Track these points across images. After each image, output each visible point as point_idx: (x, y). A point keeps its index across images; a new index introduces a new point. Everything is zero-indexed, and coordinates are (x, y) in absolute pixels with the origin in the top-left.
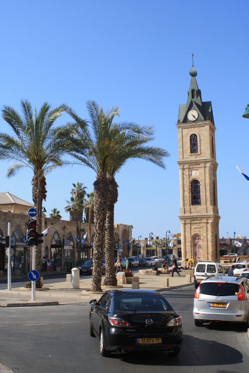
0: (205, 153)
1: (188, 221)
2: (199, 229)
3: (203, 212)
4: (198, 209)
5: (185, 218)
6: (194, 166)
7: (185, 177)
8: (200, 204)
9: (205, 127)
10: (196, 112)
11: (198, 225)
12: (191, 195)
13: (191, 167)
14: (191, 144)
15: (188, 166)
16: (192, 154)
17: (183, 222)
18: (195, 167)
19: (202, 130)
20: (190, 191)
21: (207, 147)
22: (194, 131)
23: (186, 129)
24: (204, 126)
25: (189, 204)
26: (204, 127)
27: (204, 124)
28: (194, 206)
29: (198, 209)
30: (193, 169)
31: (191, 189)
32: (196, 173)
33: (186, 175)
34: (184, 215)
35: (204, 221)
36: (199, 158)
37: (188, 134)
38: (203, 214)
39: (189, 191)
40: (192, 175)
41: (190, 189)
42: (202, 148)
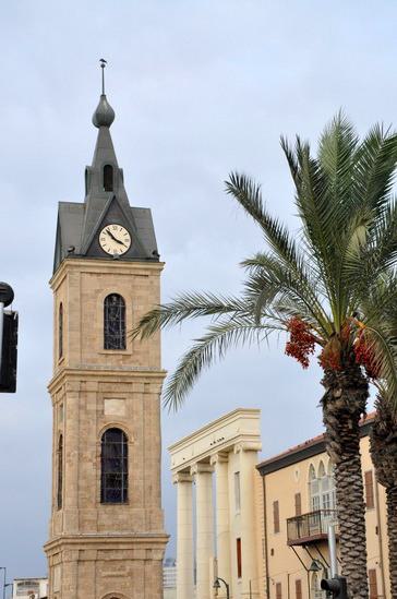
0: (148, 352)
1: (91, 554)
2: (120, 580)
3: (135, 528)
5: (83, 544)
6: (114, 386)
7: (83, 417)
8: (126, 500)
9: (152, 278)
10: (125, 231)
11: (118, 566)
12: (99, 472)
13: (104, 387)
14: (105, 325)
16: (111, 352)
17: (75, 556)
18: (117, 390)
20: (99, 459)
22: (119, 286)
23: (95, 277)
25: (94, 501)
26: (147, 280)
27: (146, 269)
28: (110, 508)
29: (121, 517)
30: (109, 395)
31: (102, 455)
32: (118, 410)
33: (87, 413)
34: (76, 532)
35: (140, 554)
36: (128, 366)
37: (98, 291)
40: (106, 413)
41: (99, 454)
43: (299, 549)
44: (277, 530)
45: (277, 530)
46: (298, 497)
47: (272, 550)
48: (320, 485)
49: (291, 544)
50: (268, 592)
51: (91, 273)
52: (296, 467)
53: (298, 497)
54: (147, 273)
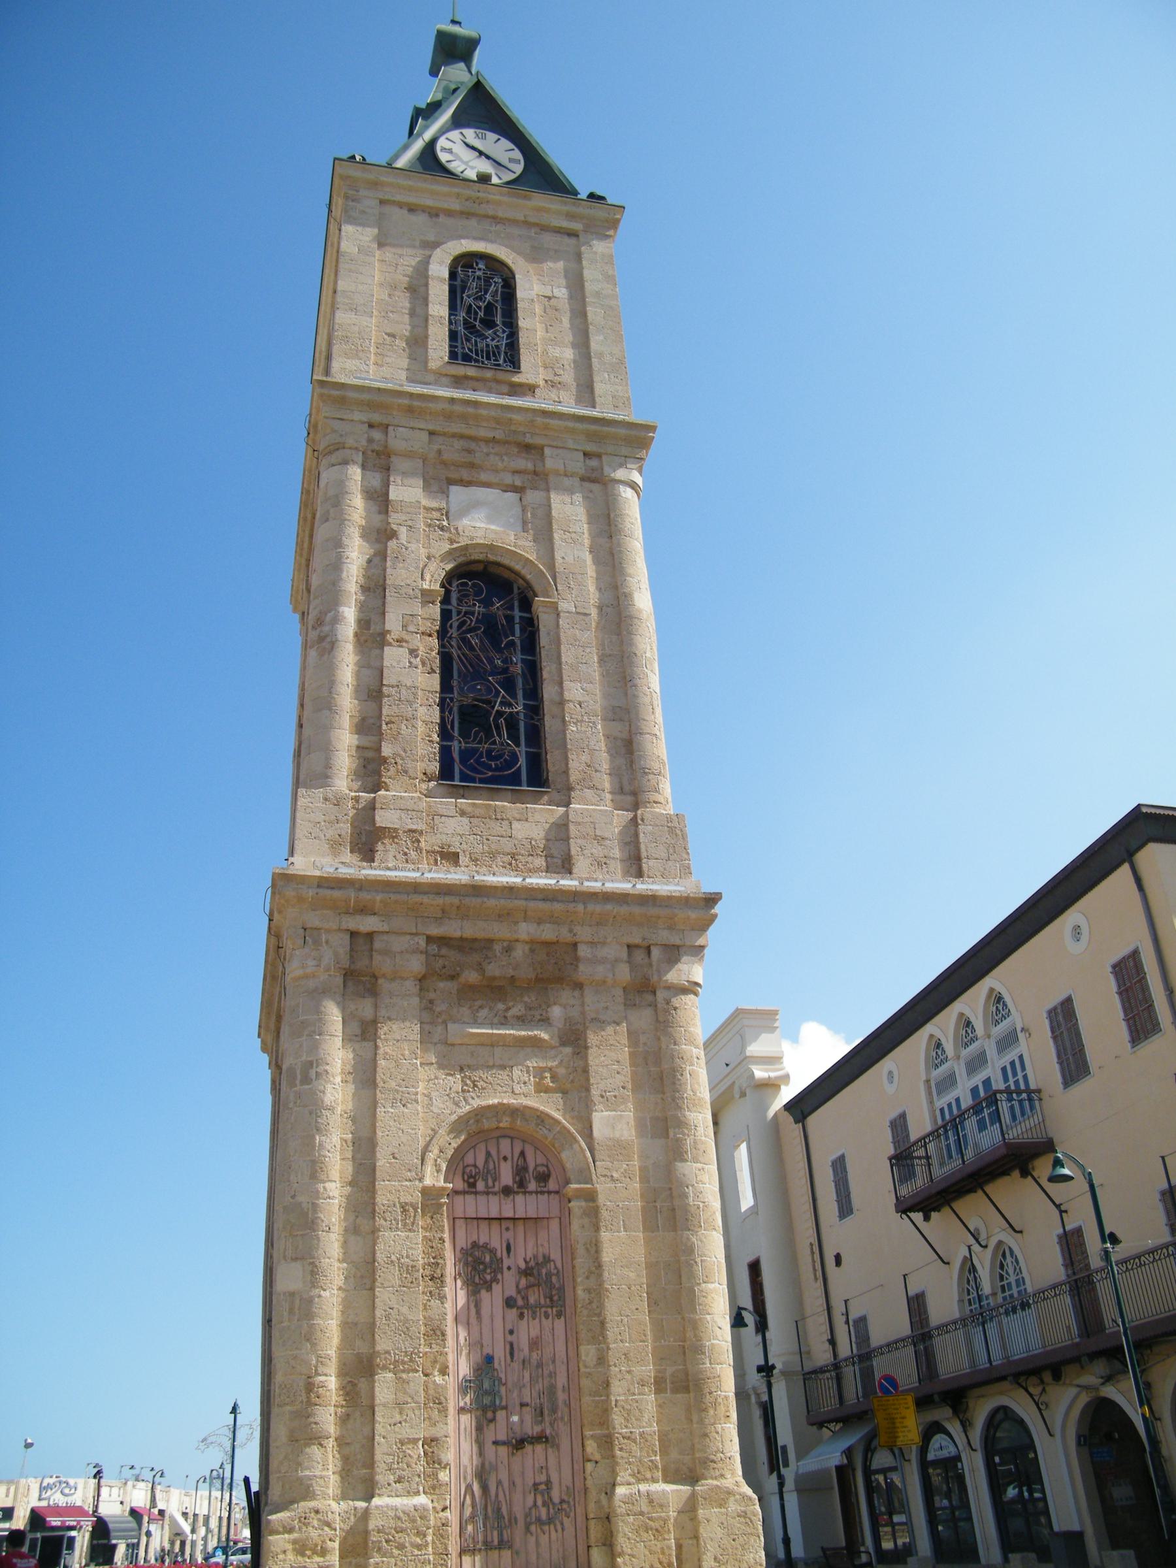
3: (581, 865)
4: (521, 830)
12: (435, 681)
15: (425, 436)
16: (471, 371)
19: (556, 251)
21: (600, 355)
23: (420, 219)
24: (573, 234)
29: (521, 830)
30: (465, 474)
31: (443, 634)
34: (349, 867)
38: (595, 886)
39: (417, 641)
42: (555, 352)
43: (918, 1217)
44: (845, 1208)
45: (845, 1208)
46: (899, 1125)
47: (838, 1260)
48: (960, 1071)
49: (905, 1208)
50: (832, 1342)
51: (412, 209)
52: (887, 1064)
53: (899, 1125)
54: (577, 226)
